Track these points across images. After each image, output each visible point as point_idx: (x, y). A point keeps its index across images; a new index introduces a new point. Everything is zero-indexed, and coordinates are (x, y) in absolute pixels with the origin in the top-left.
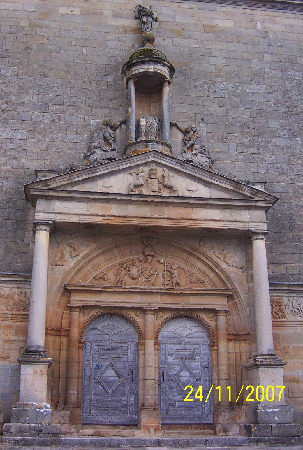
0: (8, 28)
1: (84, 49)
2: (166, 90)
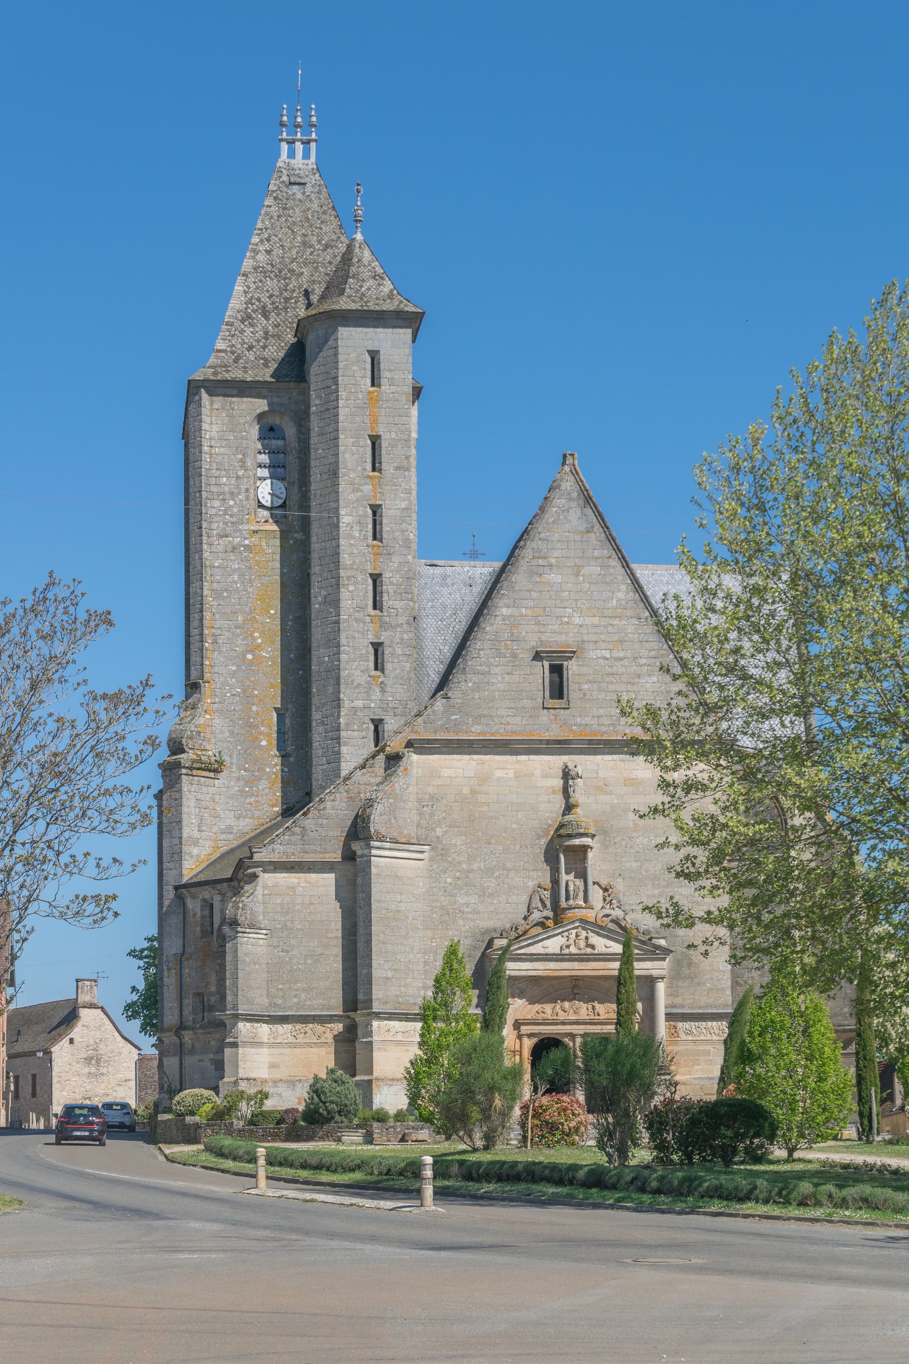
0: (453, 796)
1: (520, 813)
2: (590, 855)
